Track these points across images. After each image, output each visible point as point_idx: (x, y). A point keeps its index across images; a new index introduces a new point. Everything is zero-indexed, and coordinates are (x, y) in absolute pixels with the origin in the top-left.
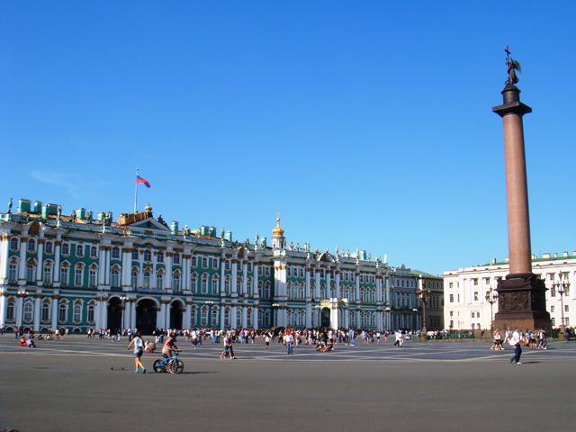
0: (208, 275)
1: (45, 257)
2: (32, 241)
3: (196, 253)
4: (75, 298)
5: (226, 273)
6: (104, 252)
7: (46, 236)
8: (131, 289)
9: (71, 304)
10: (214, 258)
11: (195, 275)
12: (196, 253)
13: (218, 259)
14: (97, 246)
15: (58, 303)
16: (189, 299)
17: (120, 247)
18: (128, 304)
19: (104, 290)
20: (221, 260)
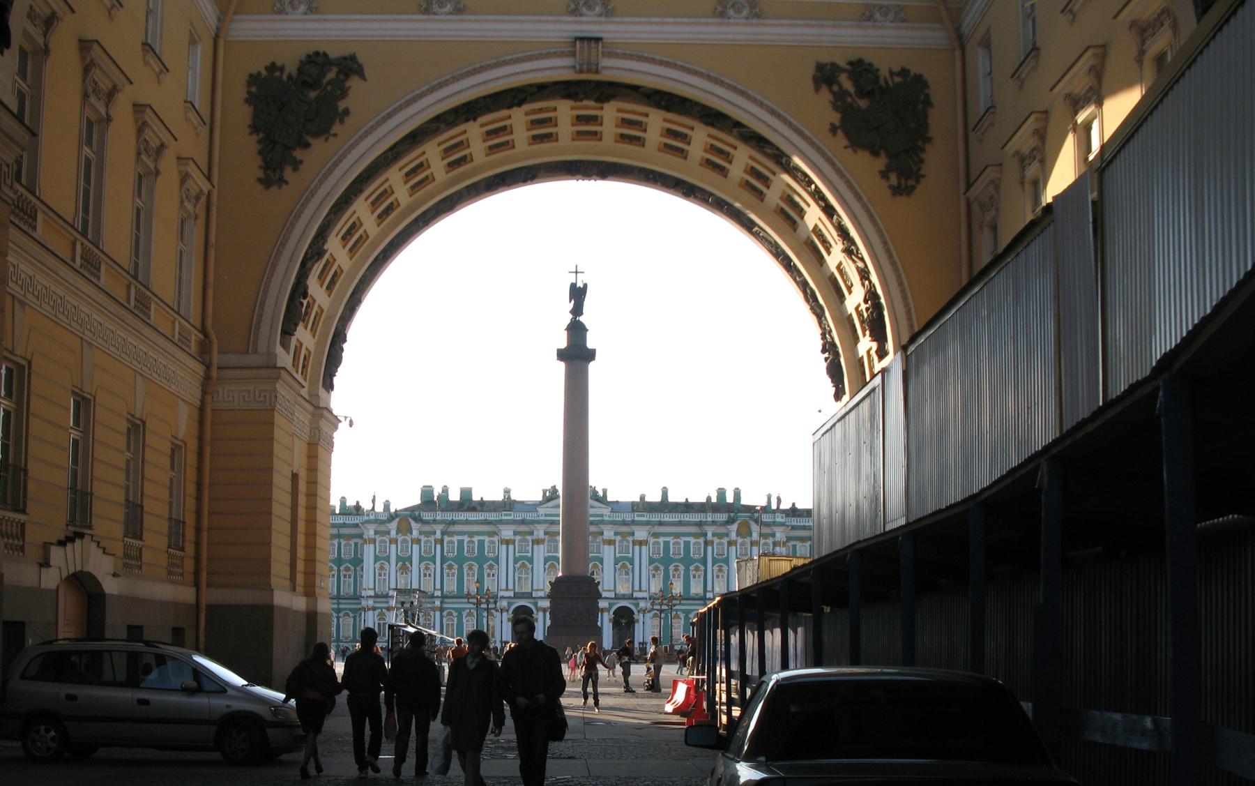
0: (682, 568)
1: (421, 559)
2: (405, 541)
3: (656, 535)
4: (464, 609)
5: (715, 561)
6: (504, 547)
7: (421, 533)
8: (541, 594)
9: (460, 617)
10: (692, 540)
11: (657, 569)
12: (656, 535)
13: (701, 540)
14: (496, 539)
15: (442, 617)
16: (642, 604)
17: (529, 538)
18: (541, 614)
19: (502, 597)
20: (706, 543)
